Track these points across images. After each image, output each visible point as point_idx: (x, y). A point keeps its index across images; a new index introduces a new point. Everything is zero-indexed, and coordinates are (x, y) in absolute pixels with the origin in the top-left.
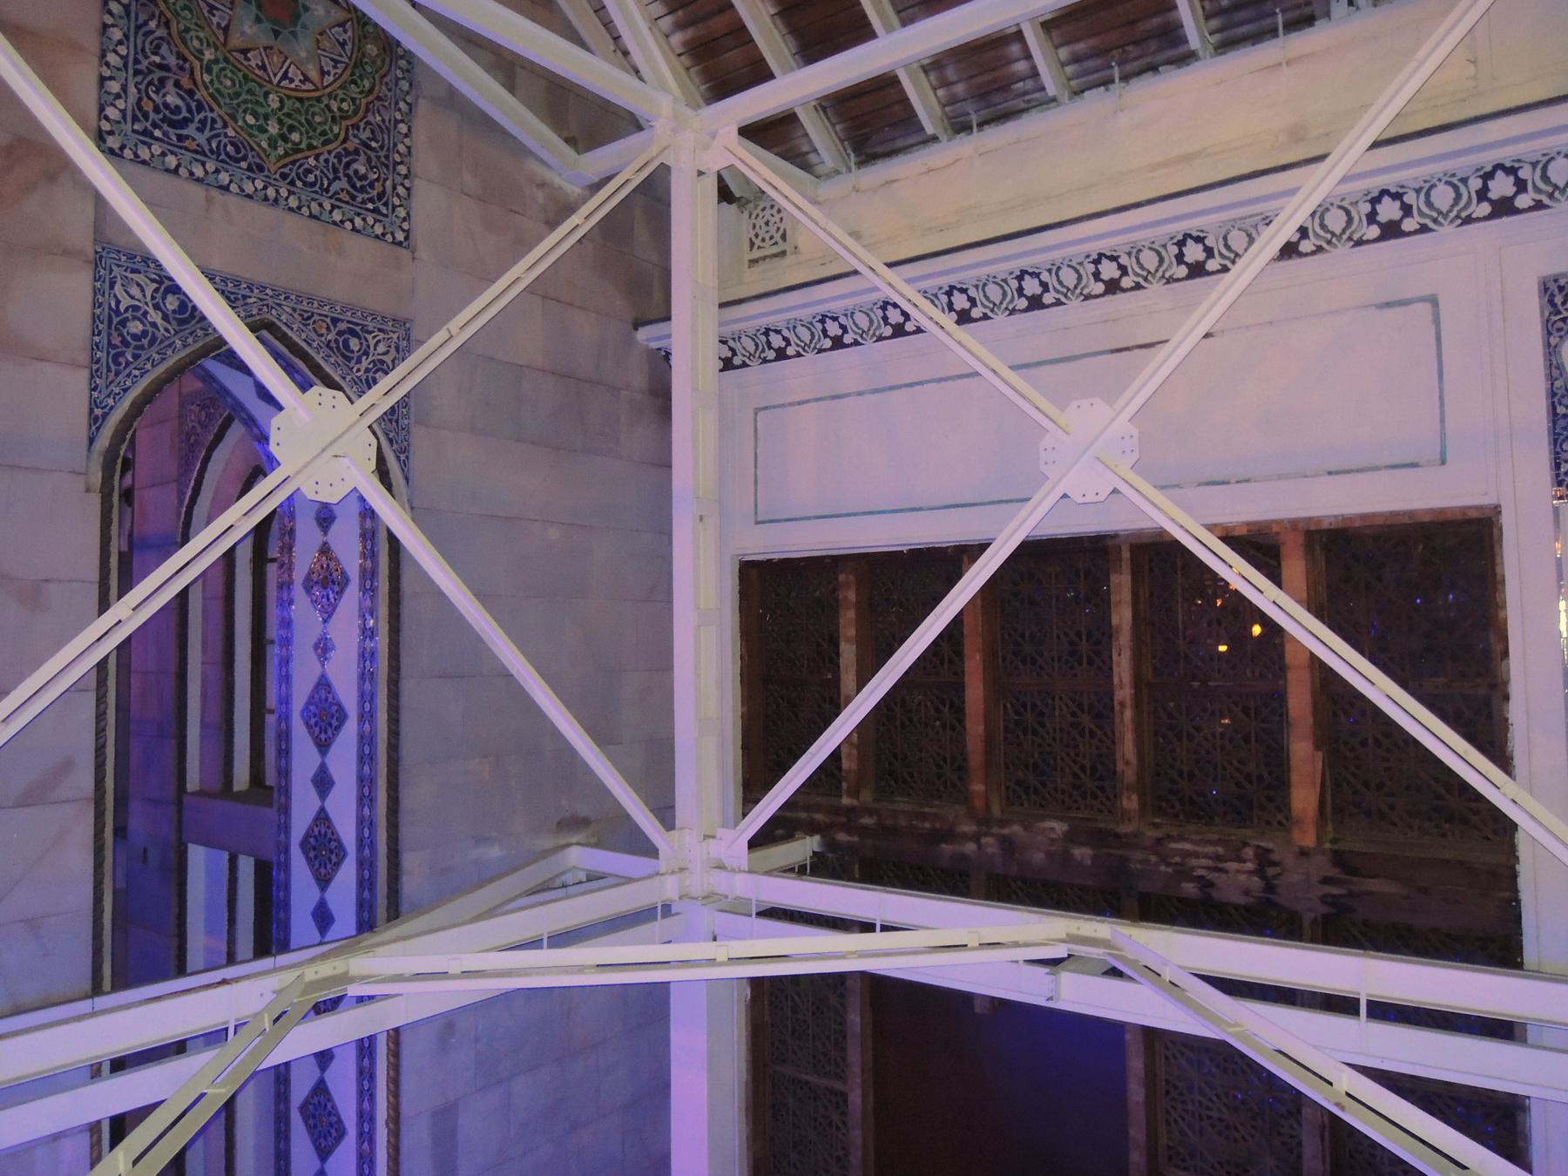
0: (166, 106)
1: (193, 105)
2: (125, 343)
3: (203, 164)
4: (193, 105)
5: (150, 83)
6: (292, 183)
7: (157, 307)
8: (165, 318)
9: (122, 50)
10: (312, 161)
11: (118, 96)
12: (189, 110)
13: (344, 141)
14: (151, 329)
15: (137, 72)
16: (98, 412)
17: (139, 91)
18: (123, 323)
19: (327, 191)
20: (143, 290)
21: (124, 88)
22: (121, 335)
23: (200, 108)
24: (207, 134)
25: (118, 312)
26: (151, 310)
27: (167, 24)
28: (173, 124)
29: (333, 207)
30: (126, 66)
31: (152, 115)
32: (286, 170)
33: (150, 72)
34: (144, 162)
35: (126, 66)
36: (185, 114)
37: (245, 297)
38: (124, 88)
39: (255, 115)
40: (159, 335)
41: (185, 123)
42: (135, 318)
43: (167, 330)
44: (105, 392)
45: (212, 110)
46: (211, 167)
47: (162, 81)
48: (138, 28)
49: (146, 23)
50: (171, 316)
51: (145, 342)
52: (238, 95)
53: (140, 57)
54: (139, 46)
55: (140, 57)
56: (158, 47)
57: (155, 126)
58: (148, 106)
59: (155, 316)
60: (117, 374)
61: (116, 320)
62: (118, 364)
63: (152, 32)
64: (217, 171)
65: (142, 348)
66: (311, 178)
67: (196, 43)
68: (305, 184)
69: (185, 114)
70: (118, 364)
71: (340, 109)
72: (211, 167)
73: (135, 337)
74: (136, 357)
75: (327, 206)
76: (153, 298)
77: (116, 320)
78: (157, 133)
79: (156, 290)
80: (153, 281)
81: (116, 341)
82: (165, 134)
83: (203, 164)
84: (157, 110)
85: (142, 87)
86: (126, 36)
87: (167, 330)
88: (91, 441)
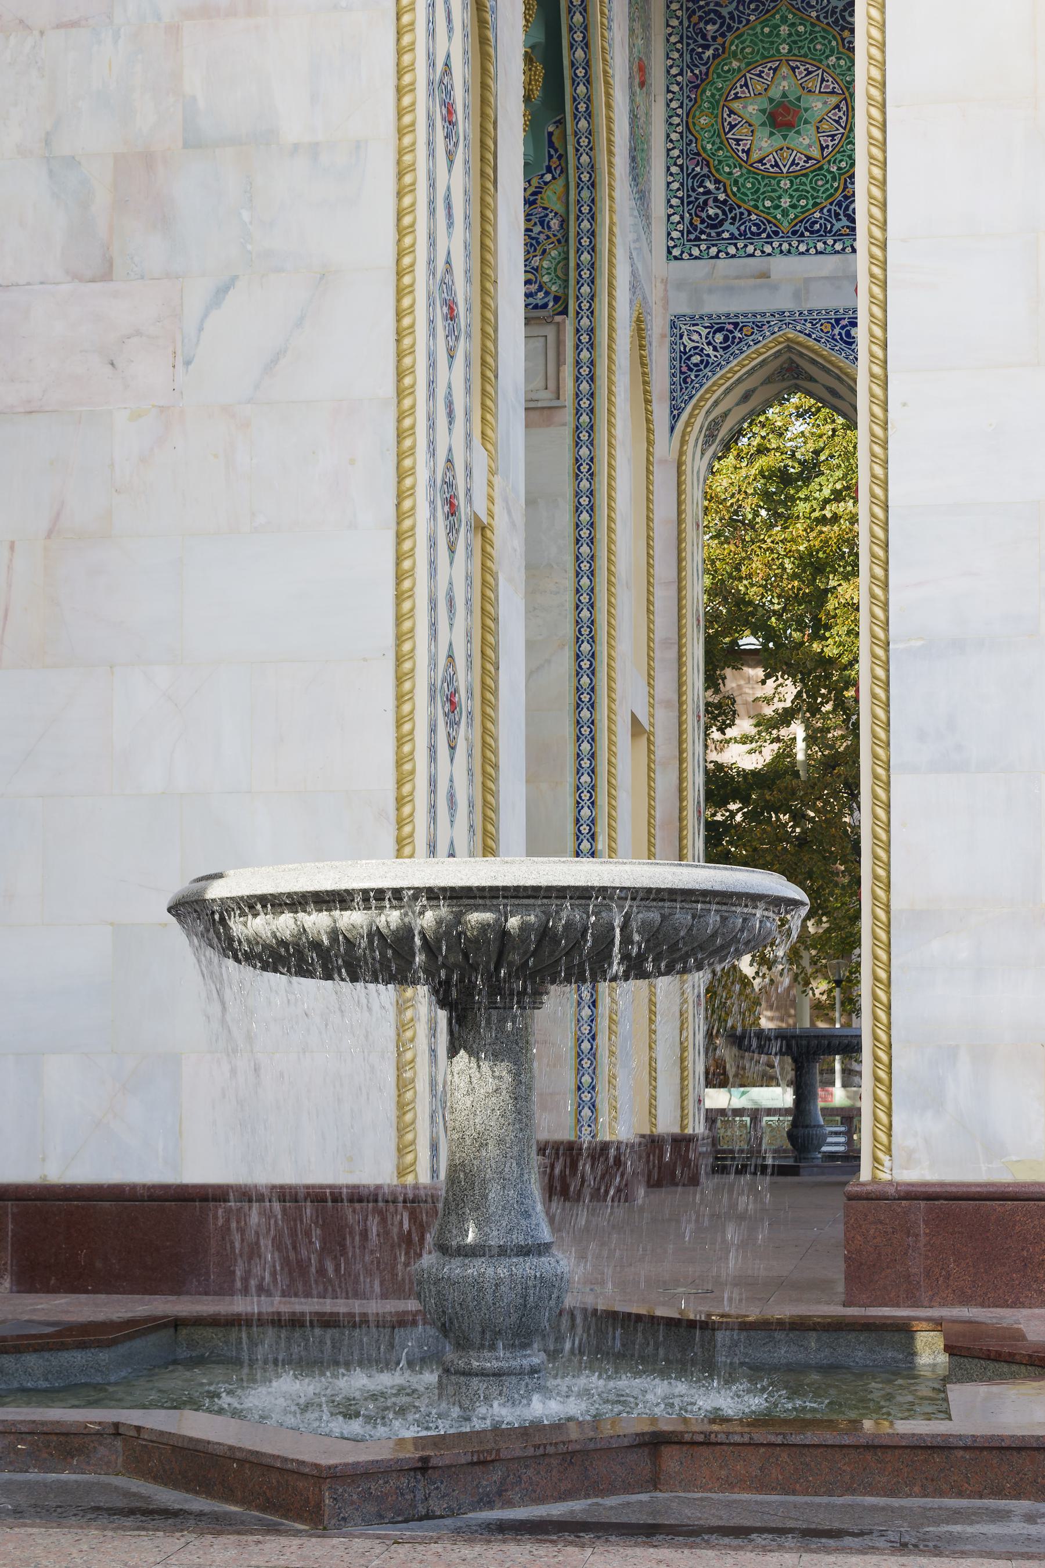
0: (709, 217)
1: (727, 209)
2: (691, 370)
3: (735, 245)
4: (727, 209)
5: (698, 206)
6: (802, 235)
7: (709, 344)
8: (715, 349)
10: (817, 215)
12: (724, 213)
13: (843, 191)
14: (705, 358)
15: (689, 203)
16: (676, 412)
17: (691, 215)
18: (689, 358)
19: (830, 231)
20: (700, 335)
21: (682, 217)
22: (688, 366)
23: (731, 210)
24: (737, 224)
25: (685, 353)
26: (706, 347)
27: (708, 165)
28: (713, 227)
29: (835, 241)
30: (682, 203)
31: (699, 226)
32: (797, 228)
33: (697, 199)
34: (696, 258)
36: (721, 217)
37: (768, 322)
38: (682, 217)
39: (772, 200)
40: (711, 361)
41: (721, 223)
42: (696, 354)
43: (716, 356)
44: (679, 401)
45: (739, 207)
46: (740, 245)
47: (705, 202)
48: (688, 175)
50: (718, 346)
51: (702, 367)
52: (756, 192)
53: (691, 193)
54: (690, 185)
55: (691, 193)
56: (703, 181)
57: (702, 232)
58: (697, 221)
59: (709, 350)
60: (687, 388)
61: (684, 357)
62: (685, 382)
64: (746, 246)
65: (701, 370)
66: (817, 227)
67: (727, 169)
68: (812, 232)
69: (721, 217)
70: (685, 382)
71: (839, 169)
72: (740, 245)
73: (696, 365)
74: (696, 376)
75: (830, 242)
76: (707, 338)
77: (684, 357)
78: (703, 237)
79: (709, 333)
80: (706, 327)
81: (685, 369)
82: (709, 235)
83: (735, 245)
84: (703, 222)
85: (693, 211)
87: (716, 356)
88: (672, 429)
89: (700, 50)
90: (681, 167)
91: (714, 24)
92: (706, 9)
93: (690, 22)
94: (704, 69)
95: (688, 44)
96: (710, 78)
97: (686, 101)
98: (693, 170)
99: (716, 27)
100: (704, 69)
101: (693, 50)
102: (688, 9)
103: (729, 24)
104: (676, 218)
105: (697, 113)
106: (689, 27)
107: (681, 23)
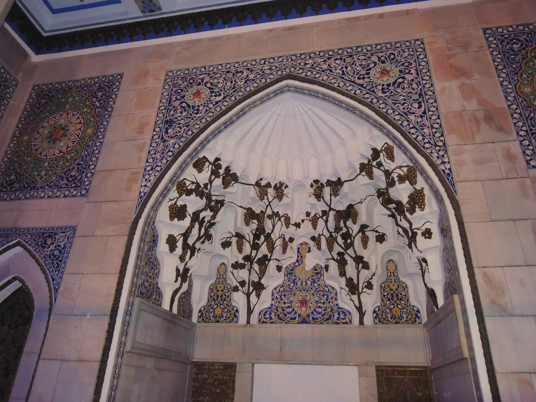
9: (524, 128)
11: (529, 145)
21: (530, 141)
30: (528, 133)
35: (528, 133)
48: (527, 118)
49: (529, 115)
53: (532, 128)
54: (530, 124)
55: (532, 128)
63: (533, 118)
86: (524, 123)
89: (513, 57)
90: (520, 114)
91: (517, 44)
92: (510, 38)
93: (503, 45)
94: (518, 65)
95: (504, 55)
96: (523, 69)
97: (512, 81)
98: (529, 115)
99: (519, 46)
100: (518, 65)
101: (508, 57)
102: (499, 39)
103: (526, 44)
104: (526, 143)
105: (521, 86)
106: (502, 47)
107: (497, 46)
